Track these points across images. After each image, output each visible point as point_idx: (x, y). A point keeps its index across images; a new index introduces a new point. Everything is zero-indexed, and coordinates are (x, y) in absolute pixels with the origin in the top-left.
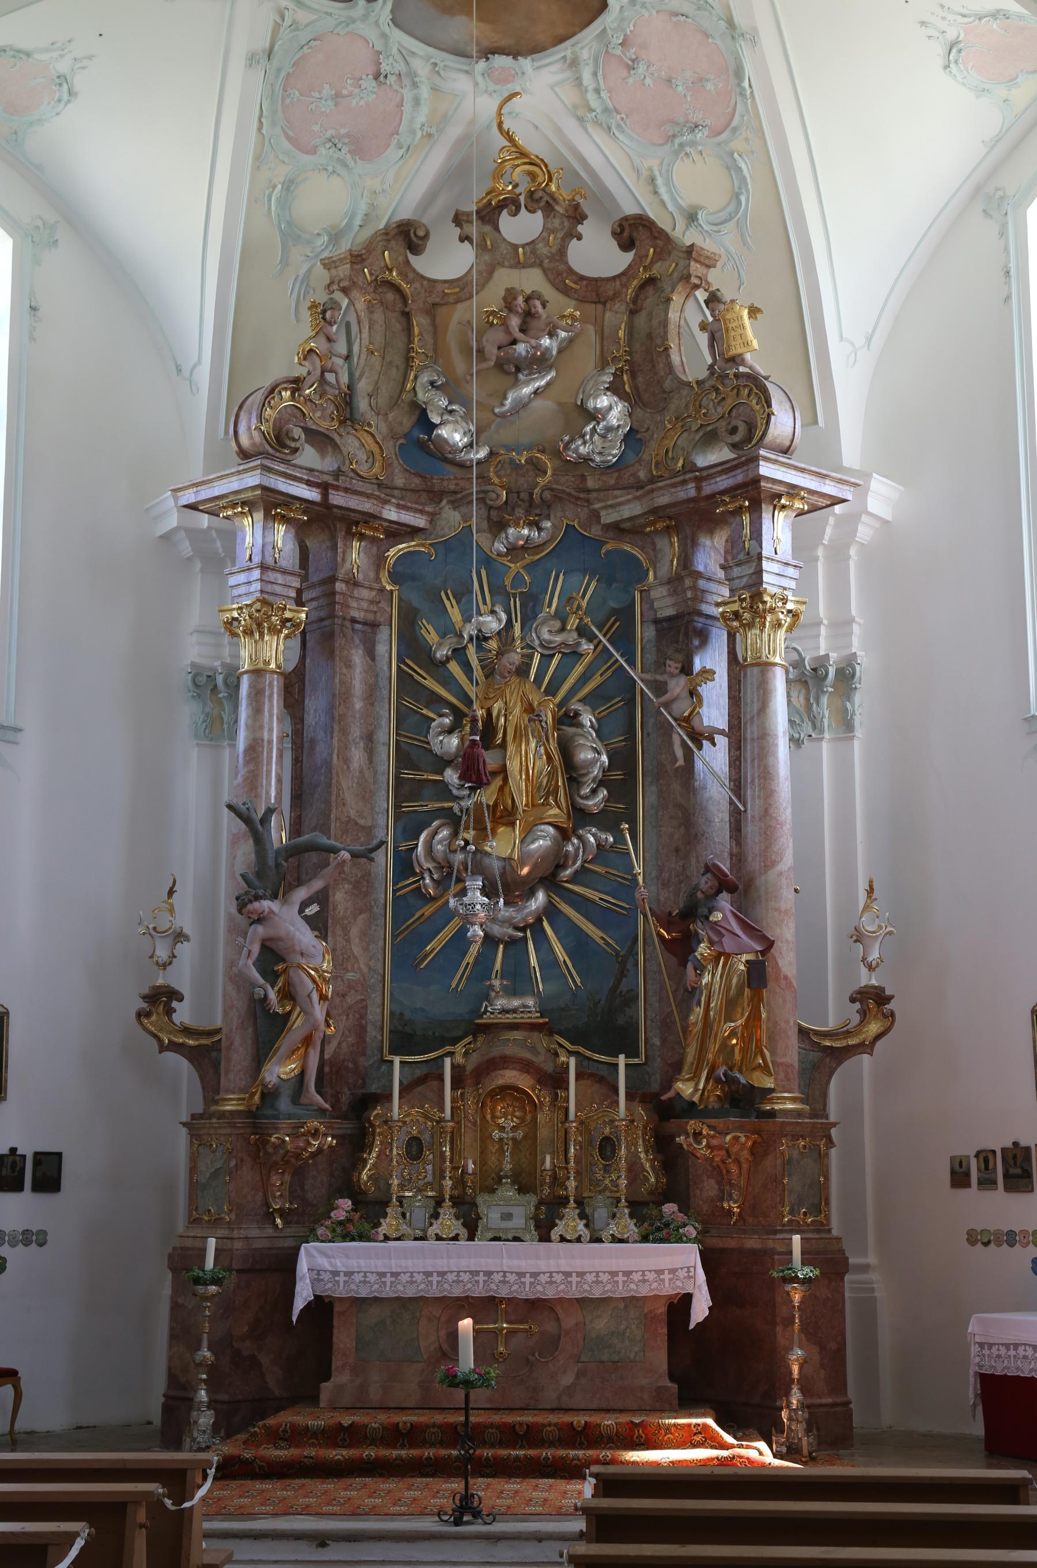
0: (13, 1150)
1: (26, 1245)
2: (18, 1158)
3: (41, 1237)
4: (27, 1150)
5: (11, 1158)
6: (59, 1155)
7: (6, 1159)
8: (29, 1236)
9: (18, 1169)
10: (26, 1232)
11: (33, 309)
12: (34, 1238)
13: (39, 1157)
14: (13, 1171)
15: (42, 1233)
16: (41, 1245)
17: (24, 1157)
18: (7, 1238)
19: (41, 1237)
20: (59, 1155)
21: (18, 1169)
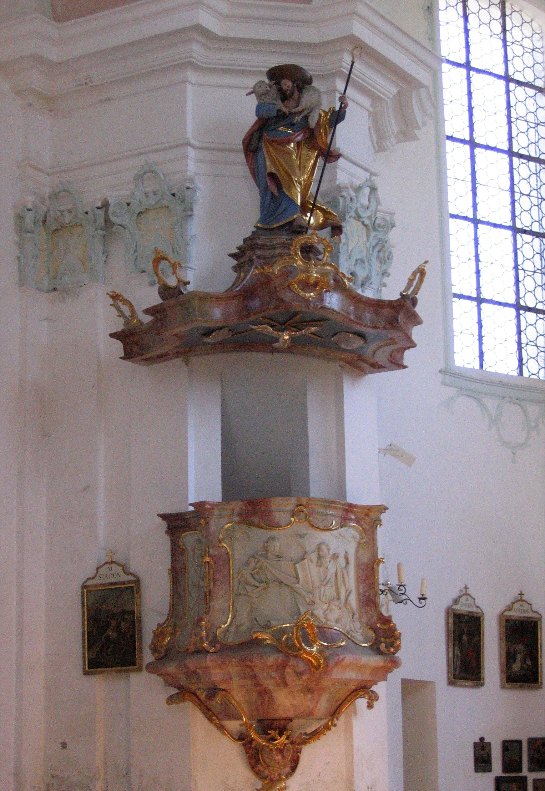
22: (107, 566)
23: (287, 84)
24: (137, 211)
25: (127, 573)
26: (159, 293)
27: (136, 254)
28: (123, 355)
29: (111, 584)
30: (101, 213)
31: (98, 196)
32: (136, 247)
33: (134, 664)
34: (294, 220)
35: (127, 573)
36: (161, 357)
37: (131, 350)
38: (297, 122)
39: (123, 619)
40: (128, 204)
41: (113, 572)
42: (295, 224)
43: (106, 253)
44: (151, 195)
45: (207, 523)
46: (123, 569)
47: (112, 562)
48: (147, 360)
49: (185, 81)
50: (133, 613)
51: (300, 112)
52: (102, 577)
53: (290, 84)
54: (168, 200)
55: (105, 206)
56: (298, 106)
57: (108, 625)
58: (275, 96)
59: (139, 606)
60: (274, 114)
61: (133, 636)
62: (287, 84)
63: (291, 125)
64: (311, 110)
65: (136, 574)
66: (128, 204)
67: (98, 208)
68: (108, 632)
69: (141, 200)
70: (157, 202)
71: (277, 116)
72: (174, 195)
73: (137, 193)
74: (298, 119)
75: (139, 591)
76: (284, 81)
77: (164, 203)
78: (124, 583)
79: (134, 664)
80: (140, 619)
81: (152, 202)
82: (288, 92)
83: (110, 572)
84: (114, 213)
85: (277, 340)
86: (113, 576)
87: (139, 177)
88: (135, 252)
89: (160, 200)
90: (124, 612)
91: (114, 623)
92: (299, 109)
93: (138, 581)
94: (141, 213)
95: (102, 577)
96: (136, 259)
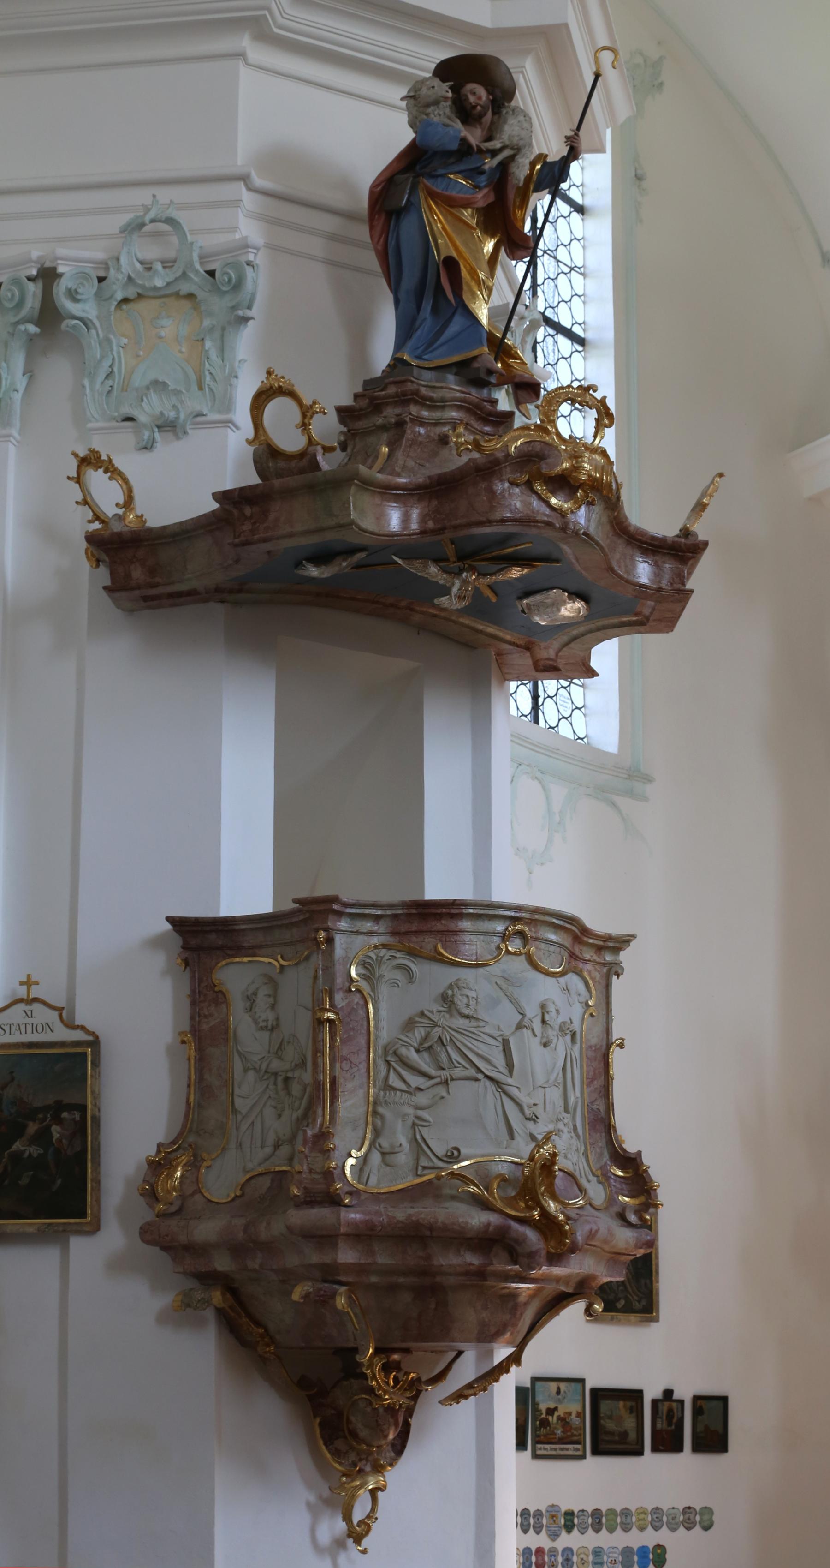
0: (668, 1394)
1: (688, 1529)
2: (674, 1405)
3: (706, 1517)
4: (685, 1392)
5: (666, 1404)
6: (724, 1400)
7: (660, 1405)
8: (692, 1516)
9: (675, 1420)
10: (688, 1510)
11: (639, 178)
12: (698, 1518)
13: (699, 1402)
14: (670, 1423)
15: (707, 1511)
16: (707, 1528)
17: (682, 1402)
18: (665, 1519)
19: (706, 1517)
20: (724, 1400)
21: (675, 1420)
22: (21, 1007)
23: (477, 94)
24: (119, 296)
25: (70, 1025)
26: (255, 462)
27: (110, 382)
28: (108, 583)
29: (31, 1045)
30: (34, 290)
31: (35, 254)
32: (111, 366)
33: (83, 1215)
34: (475, 358)
35: (70, 1025)
36: (178, 598)
37: (128, 576)
38: (491, 169)
39: (59, 1121)
40: (101, 280)
41: (34, 1021)
42: (476, 365)
43: (29, 372)
44: (159, 267)
45: (330, 941)
46: (61, 1016)
47: (36, 1000)
48: (145, 599)
49: (241, 55)
50: (83, 1108)
51: (494, 153)
52: (7, 1029)
53: (482, 91)
54: (196, 283)
55: (48, 276)
56: (489, 139)
57: (18, 1130)
58: (448, 111)
59: (96, 1096)
60: (455, 146)
61: (80, 1158)
62: (477, 94)
63: (474, 173)
64: (517, 150)
65: (90, 1028)
66: (101, 280)
67: (30, 279)
68: (17, 1146)
69: (133, 276)
70: (168, 284)
71: (458, 151)
72: (211, 273)
73: (123, 260)
74: (490, 163)
75: (96, 1064)
76: (471, 86)
77: (185, 288)
78: (63, 1044)
79: (83, 1215)
80: (96, 1121)
81: (159, 283)
82: (479, 108)
83: (27, 1020)
84: (72, 295)
85: (445, 591)
86: (35, 1029)
87: (135, 227)
88: (107, 377)
89: (176, 279)
90: (60, 1106)
91: (32, 1128)
92: (496, 144)
93: (95, 1043)
94: (125, 300)
95: (7, 1029)
96: (109, 392)
